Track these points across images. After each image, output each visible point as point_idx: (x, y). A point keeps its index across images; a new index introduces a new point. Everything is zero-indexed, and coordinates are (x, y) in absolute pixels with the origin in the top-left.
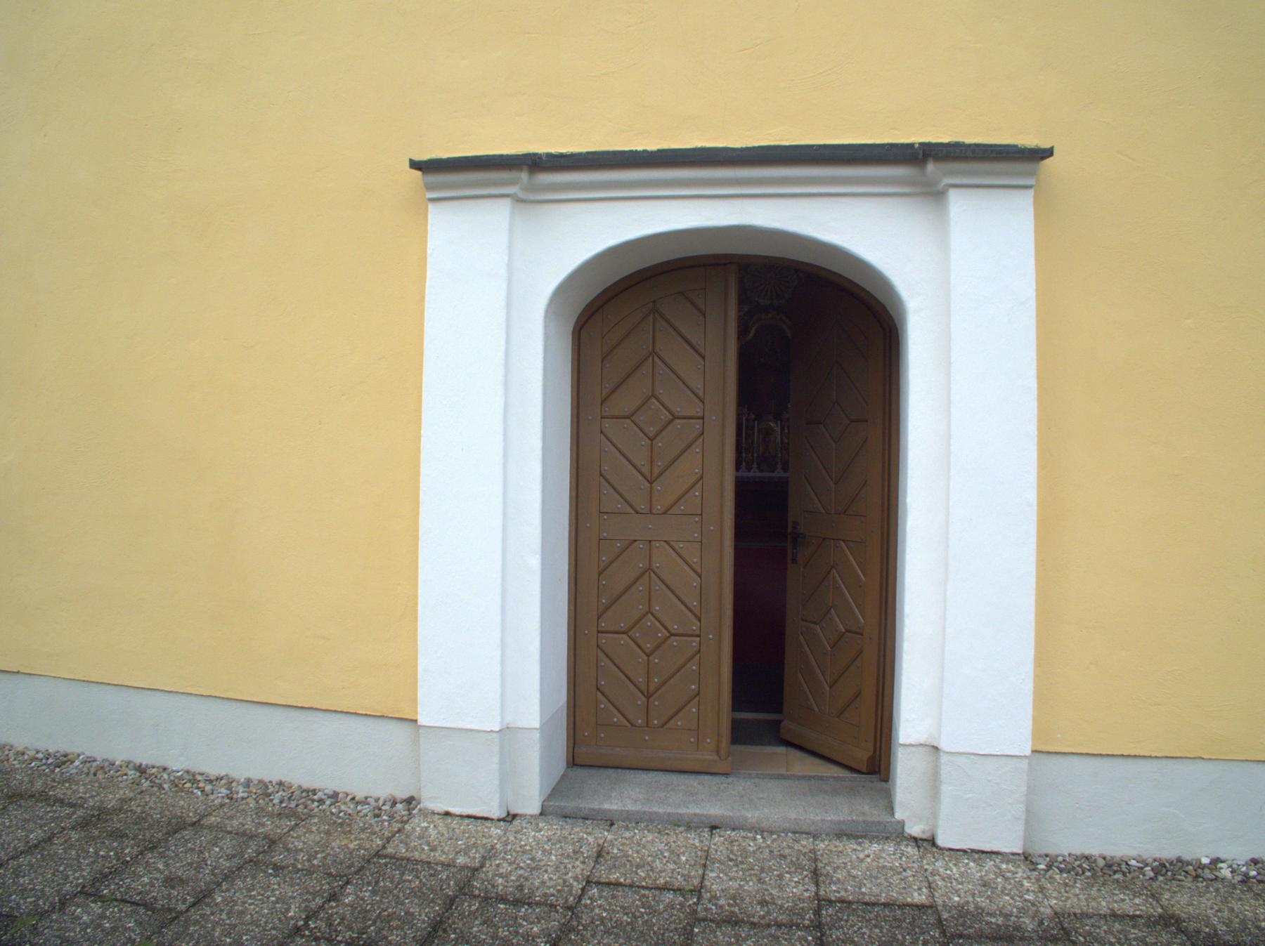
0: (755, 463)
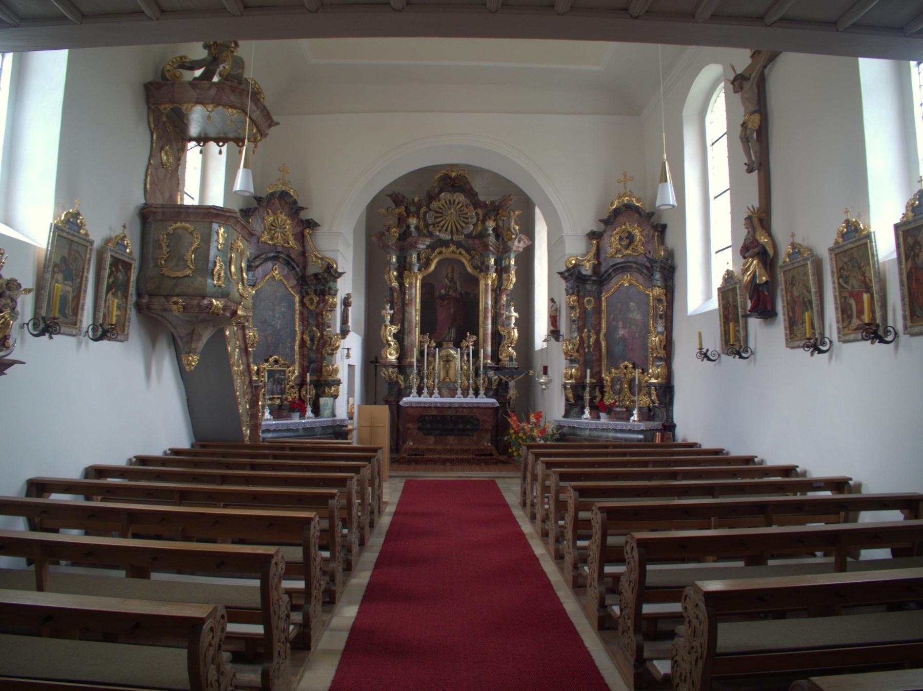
0: (436, 389)
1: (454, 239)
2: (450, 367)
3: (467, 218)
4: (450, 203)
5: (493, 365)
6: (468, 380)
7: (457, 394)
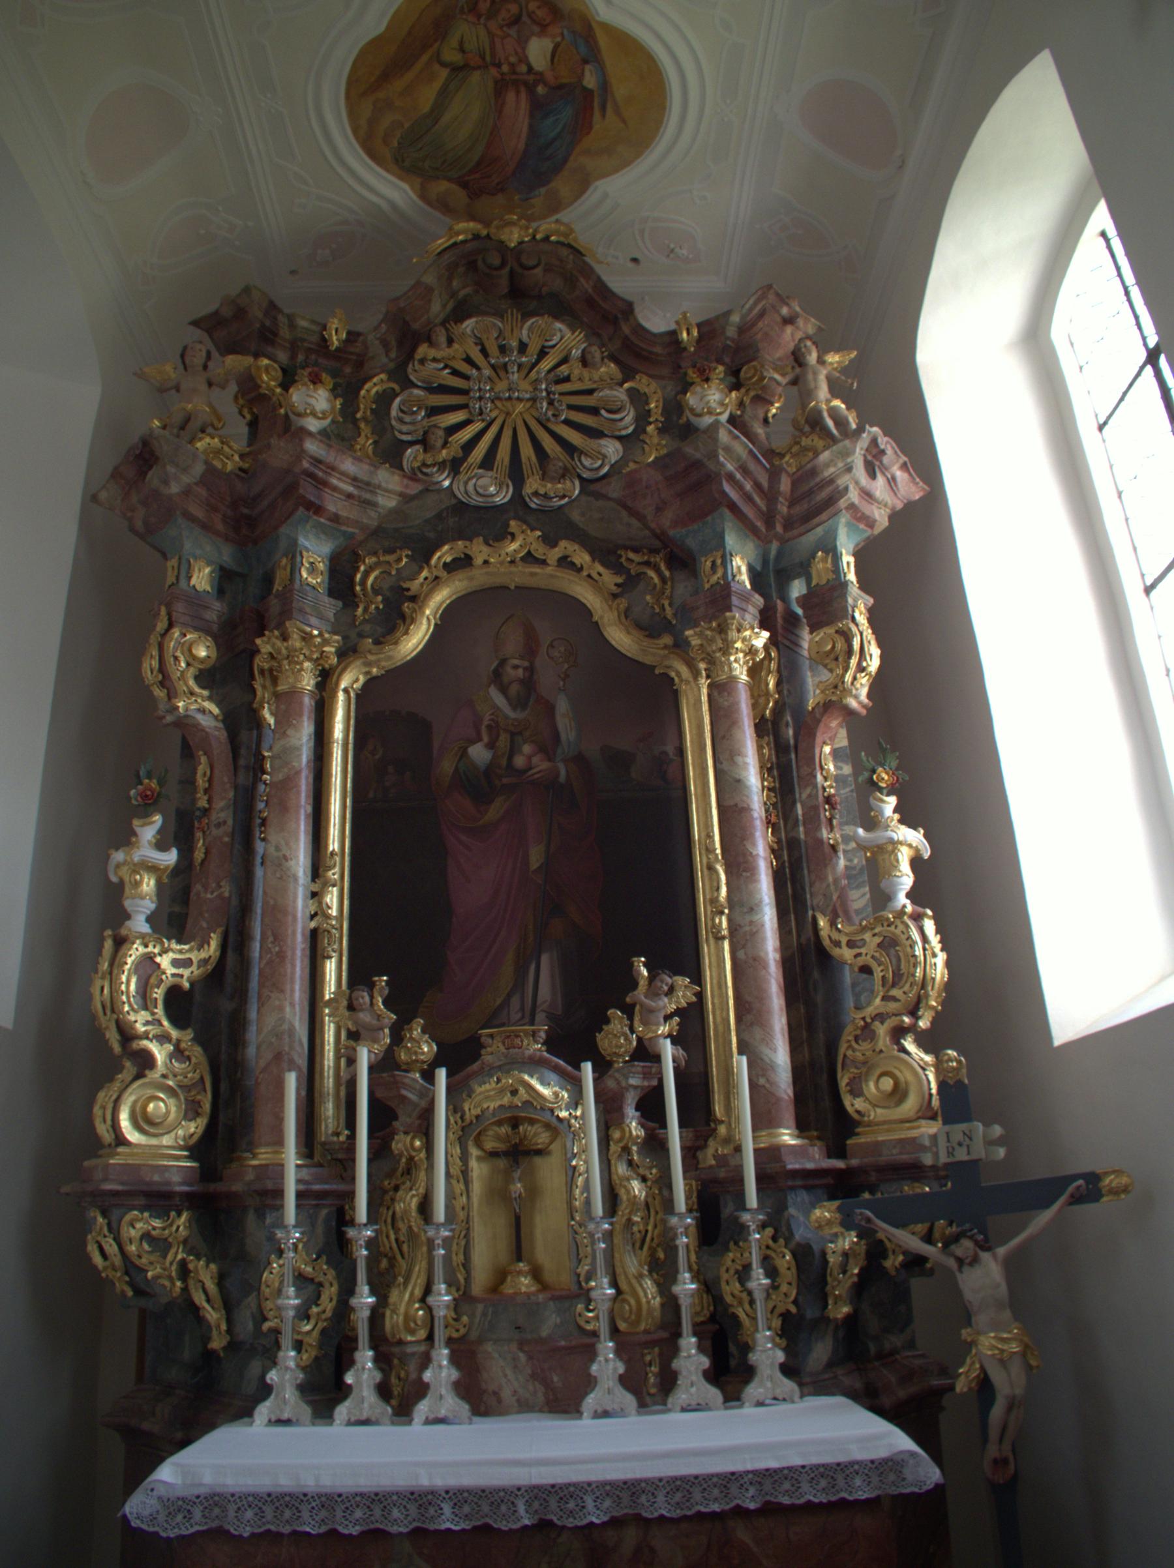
0: (442, 1354)
1: (534, 503)
2: (533, 1192)
3: (594, 411)
4: (503, 349)
5: (816, 1158)
6: (665, 1272)
7: (590, 1383)
